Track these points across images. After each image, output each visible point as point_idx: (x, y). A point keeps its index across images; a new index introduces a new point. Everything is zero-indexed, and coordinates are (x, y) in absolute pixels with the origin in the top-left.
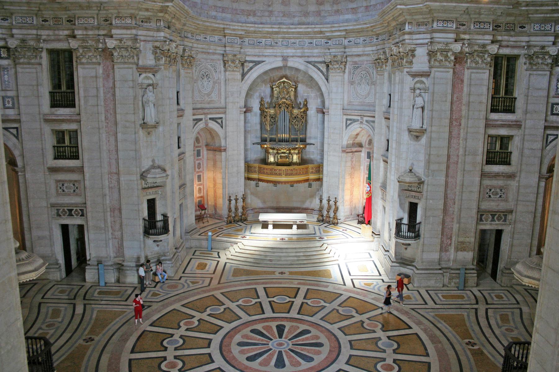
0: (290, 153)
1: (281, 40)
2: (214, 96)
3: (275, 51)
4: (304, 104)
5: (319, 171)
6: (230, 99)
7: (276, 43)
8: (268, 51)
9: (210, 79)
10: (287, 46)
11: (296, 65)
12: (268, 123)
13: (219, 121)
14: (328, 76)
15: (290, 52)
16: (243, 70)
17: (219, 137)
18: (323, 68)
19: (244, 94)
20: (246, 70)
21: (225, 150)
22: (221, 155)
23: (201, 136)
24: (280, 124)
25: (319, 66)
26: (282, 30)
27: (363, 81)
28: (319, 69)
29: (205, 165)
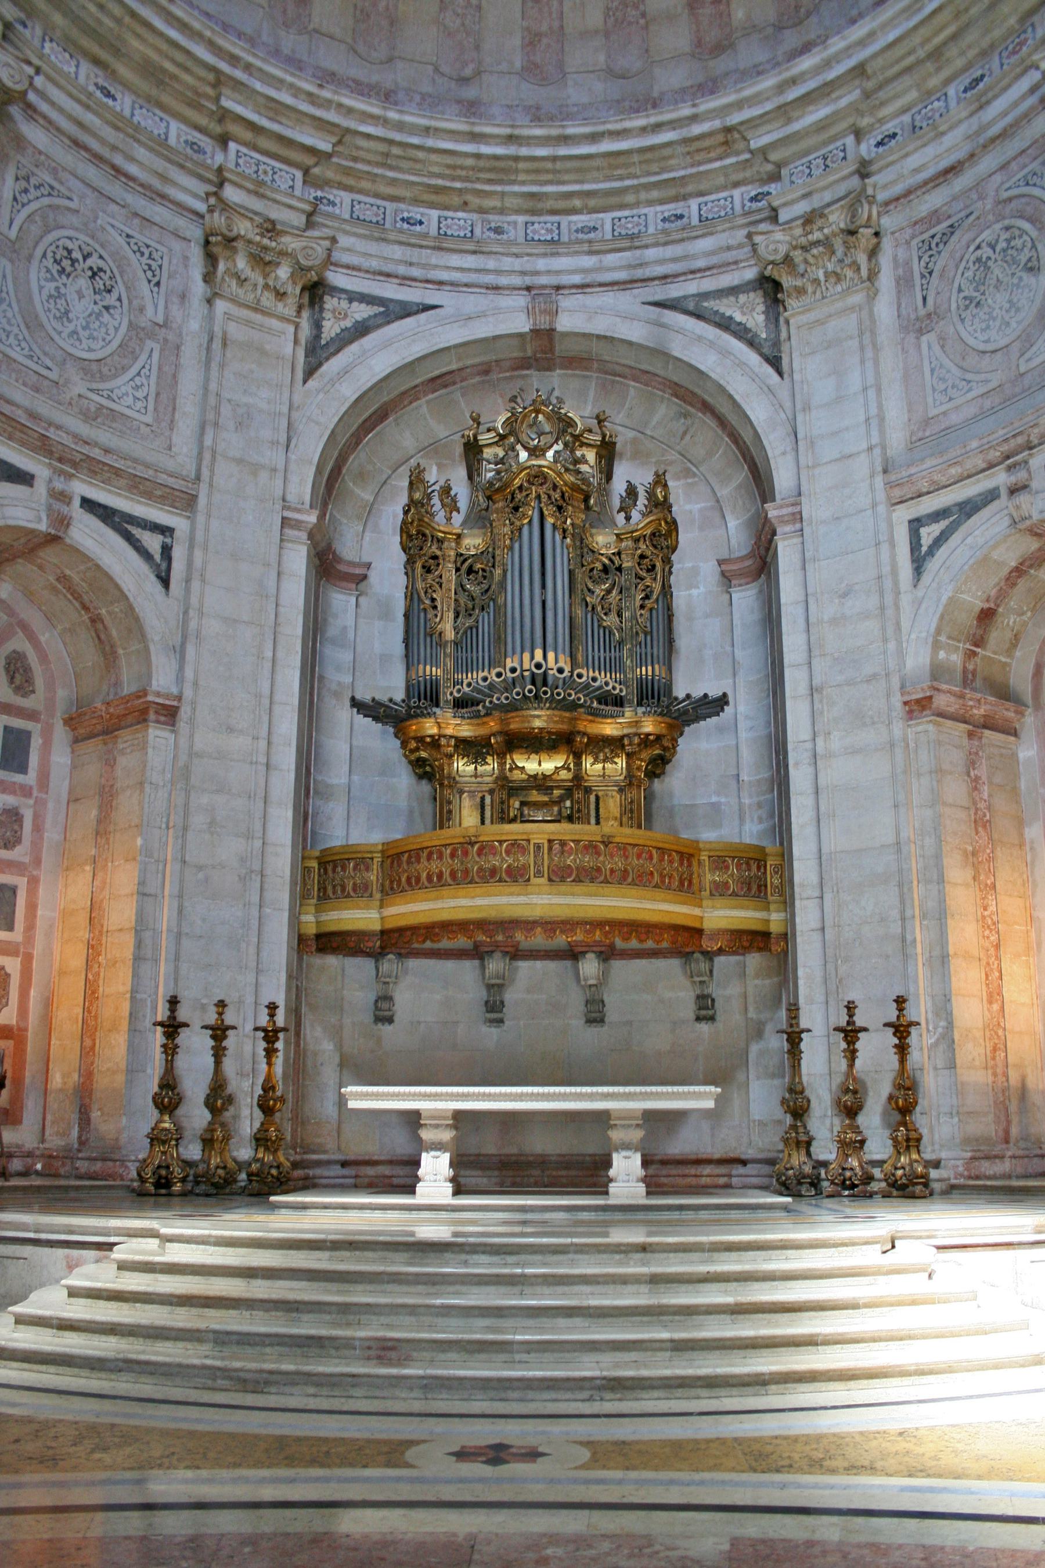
0: (578, 778)
1: (521, 219)
2: (127, 393)
3: (491, 264)
4: (651, 495)
5: (762, 887)
6: (231, 441)
7: (498, 231)
8: (455, 260)
9: (111, 300)
10: (553, 245)
11: (600, 326)
12: (445, 599)
13: (153, 542)
14: (777, 344)
15: (568, 266)
16: (317, 326)
17: (143, 637)
18: (751, 313)
19: (311, 446)
20: (331, 328)
21: (170, 714)
22: (143, 747)
23: (43, 658)
24: (517, 598)
25: (728, 308)
26: (524, 151)
27: (997, 272)
28: (725, 324)
29: (52, 834)
